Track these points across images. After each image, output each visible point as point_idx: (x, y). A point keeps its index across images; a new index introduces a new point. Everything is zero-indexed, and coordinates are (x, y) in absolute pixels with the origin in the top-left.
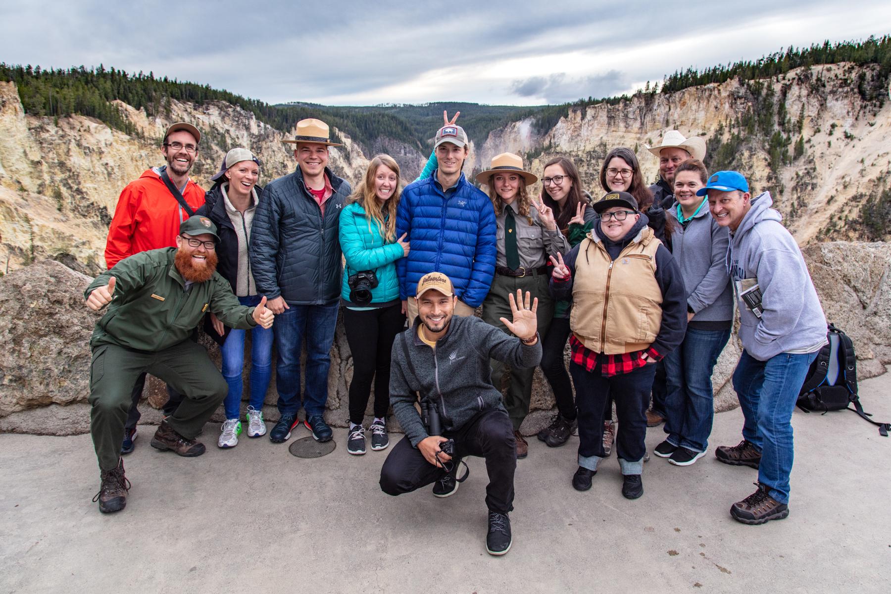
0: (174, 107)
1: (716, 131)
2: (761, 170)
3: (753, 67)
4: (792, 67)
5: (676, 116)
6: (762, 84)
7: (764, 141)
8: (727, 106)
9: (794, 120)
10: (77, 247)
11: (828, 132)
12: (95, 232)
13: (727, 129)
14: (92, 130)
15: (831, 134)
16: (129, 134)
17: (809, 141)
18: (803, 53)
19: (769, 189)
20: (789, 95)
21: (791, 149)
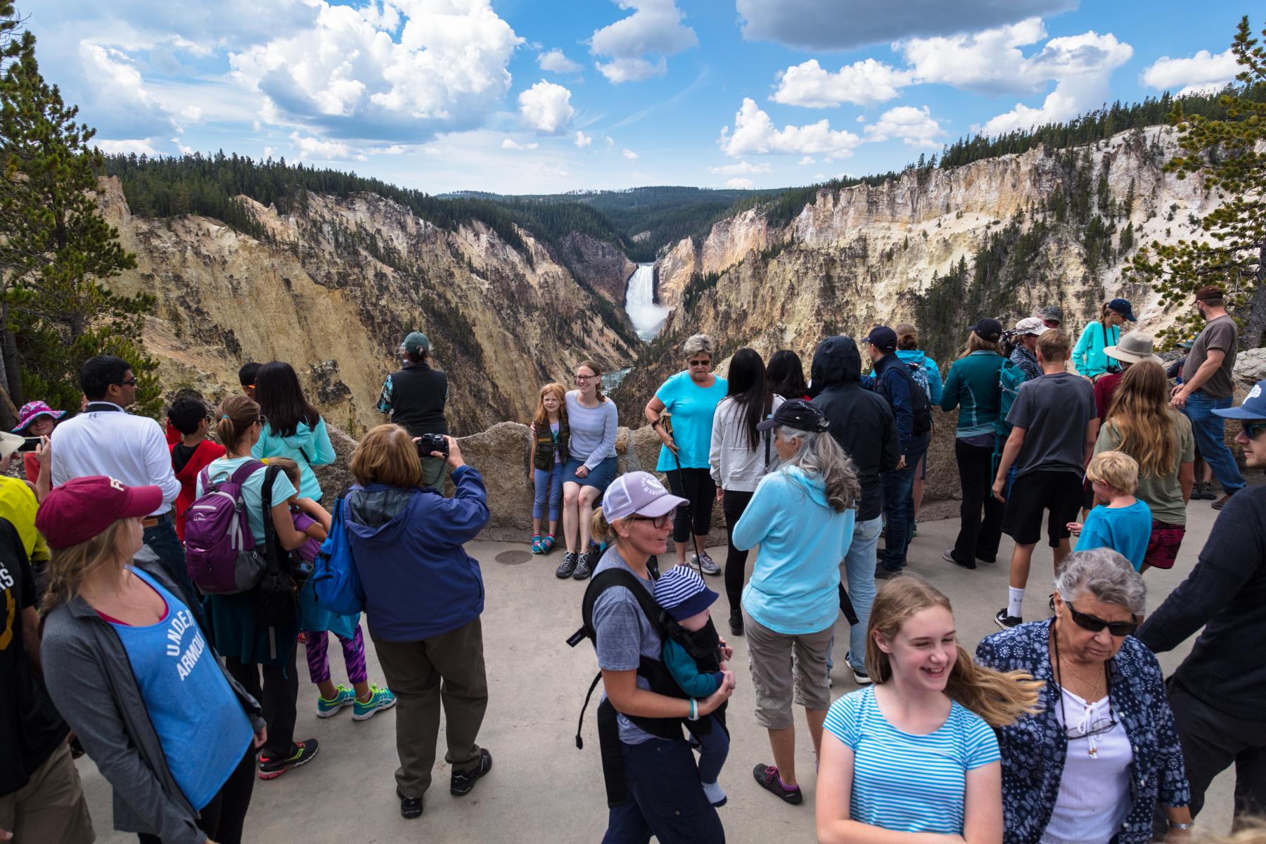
0: (311, 201)
1: (1014, 218)
2: (1075, 270)
3: (1066, 130)
4: (1118, 130)
5: (959, 200)
6: (1077, 154)
7: (1078, 231)
8: (1028, 184)
9: (1119, 200)
10: (200, 381)
11: (1167, 216)
12: (221, 363)
13: (1028, 216)
14: (213, 235)
15: (1170, 218)
16: (258, 238)
17: (1140, 228)
18: (1134, 110)
19: (1084, 294)
20: (1113, 168)
21: (1116, 241)
